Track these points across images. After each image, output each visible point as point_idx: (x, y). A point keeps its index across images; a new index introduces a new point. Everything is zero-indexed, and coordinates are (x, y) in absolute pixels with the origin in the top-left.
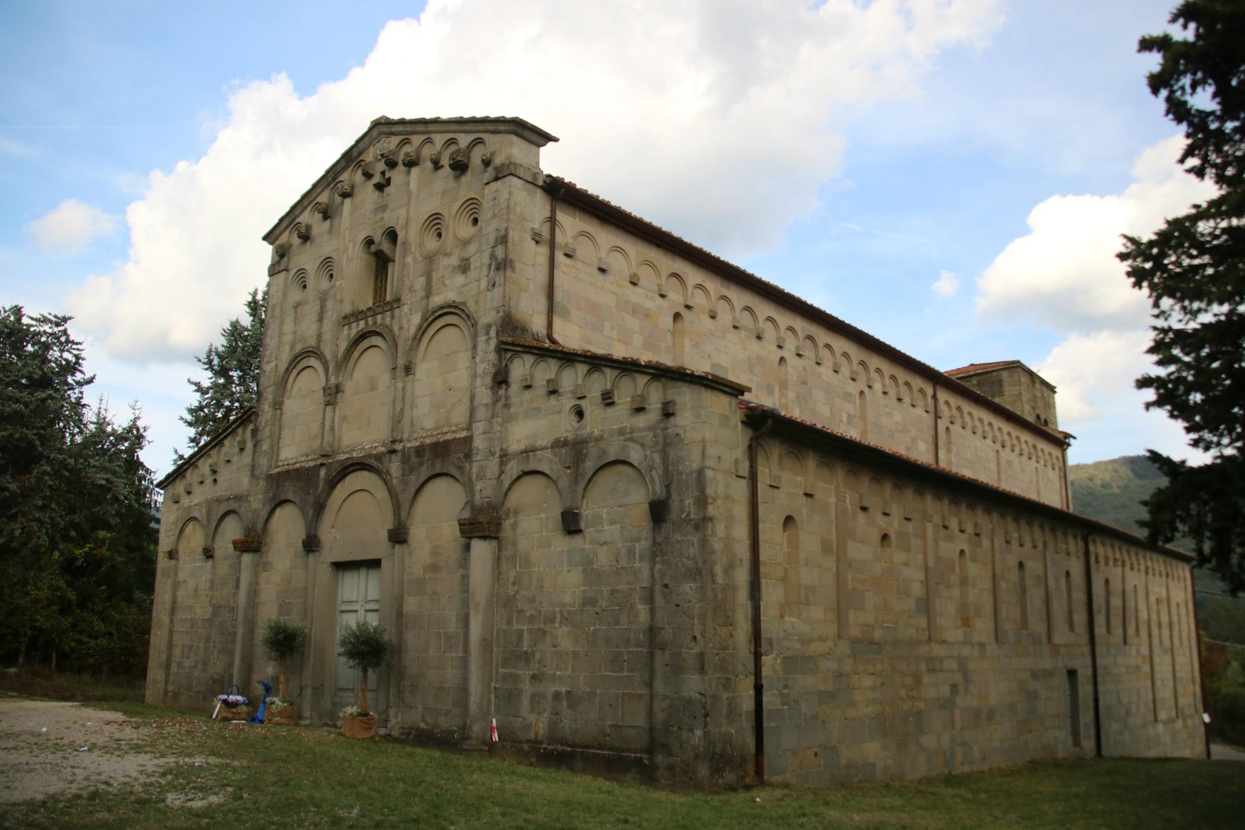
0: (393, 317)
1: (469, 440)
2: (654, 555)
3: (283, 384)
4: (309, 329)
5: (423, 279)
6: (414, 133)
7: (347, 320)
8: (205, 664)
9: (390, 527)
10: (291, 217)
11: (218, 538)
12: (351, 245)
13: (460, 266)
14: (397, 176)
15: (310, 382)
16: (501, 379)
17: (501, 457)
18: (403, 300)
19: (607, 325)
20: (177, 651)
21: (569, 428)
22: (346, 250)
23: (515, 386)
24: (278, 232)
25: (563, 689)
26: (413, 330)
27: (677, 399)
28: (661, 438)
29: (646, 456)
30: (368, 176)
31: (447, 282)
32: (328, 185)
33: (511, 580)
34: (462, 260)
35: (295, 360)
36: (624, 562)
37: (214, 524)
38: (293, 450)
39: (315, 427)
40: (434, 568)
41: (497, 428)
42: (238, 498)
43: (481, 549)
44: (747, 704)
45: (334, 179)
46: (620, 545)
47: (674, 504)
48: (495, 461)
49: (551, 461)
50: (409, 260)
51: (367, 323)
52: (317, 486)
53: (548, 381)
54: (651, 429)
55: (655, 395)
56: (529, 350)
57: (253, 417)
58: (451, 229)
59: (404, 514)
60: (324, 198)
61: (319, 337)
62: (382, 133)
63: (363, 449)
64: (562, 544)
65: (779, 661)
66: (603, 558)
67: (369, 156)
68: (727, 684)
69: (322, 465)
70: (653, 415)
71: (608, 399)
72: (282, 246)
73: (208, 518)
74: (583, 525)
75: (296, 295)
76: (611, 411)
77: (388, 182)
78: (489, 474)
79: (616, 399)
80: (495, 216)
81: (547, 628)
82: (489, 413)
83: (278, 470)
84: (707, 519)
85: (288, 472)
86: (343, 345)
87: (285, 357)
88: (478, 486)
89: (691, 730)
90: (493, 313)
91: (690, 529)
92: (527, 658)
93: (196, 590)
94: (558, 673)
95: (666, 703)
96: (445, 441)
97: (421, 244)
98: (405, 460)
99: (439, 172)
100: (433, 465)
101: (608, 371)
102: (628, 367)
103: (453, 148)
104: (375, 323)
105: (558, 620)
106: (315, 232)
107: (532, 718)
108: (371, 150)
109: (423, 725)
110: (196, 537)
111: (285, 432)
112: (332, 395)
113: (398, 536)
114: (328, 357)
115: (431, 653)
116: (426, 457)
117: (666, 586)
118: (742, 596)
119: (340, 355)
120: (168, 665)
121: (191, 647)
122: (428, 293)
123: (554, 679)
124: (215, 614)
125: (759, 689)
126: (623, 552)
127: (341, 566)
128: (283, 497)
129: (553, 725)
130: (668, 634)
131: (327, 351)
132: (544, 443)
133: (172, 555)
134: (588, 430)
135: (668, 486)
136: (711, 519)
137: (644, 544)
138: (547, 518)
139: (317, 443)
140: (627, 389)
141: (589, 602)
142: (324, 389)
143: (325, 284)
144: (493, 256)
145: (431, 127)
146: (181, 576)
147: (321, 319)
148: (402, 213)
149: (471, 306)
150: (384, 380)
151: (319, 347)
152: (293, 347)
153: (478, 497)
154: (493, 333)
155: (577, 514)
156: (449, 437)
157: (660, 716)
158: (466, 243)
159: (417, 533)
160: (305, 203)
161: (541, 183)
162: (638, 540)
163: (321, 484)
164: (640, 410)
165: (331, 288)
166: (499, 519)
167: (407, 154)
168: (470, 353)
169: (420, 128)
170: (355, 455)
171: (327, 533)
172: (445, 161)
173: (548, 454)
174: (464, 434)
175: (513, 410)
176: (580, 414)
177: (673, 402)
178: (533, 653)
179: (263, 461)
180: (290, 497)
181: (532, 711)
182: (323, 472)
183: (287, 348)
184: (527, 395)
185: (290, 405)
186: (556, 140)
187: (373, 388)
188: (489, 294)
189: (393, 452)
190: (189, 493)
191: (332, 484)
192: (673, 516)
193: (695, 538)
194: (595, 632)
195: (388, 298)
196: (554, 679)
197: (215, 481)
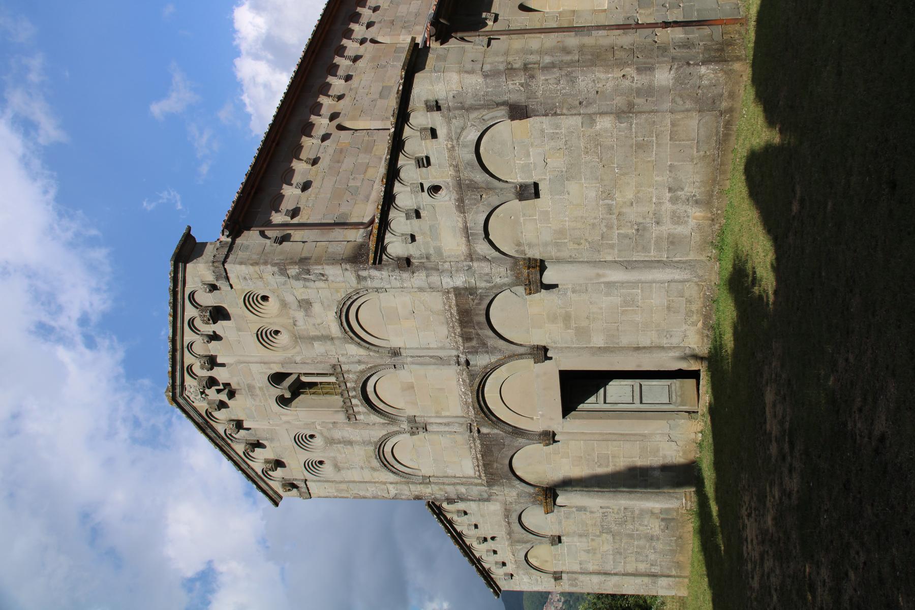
0: (348, 372)
1: (458, 291)
2: (555, 114)
4: (361, 455)
5: (316, 344)
7: (351, 415)
8: (652, 538)
9: (532, 361)
10: (257, 479)
11: (542, 532)
12: (284, 418)
13: (306, 310)
15: (405, 448)
16: (406, 263)
17: (472, 260)
18: (334, 362)
19: (352, 183)
20: (642, 567)
21: (447, 198)
22: (288, 422)
24: (270, 493)
25: (668, 195)
26: (362, 352)
27: (424, 99)
28: (457, 112)
29: (472, 125)
30: (222, 405)
31: (319, 321)
32: (229, 445)
33: (576, 246)
35: (386, 464)
37: (531, 536)
38: (464, 464)
39: (445, 441)
40: (567, 318)
41: (447, 265)
42: (507, 514)
44: (678, 34)
45: (223, 439)
46: (547, 148)
47: (513, 98)
48: (475, 265)
49: (477, 213)
50: (298, 359)
51: (354, 397)
52: (496, 434)
53: (408, 217)
54: (449, 121)
55: (419, 118)
56: (381, 238)
57: (438, 503)
58: (271, 321)
59: (521, 350)
60: (240, 448)
61: (364, 443)
62: (181, 394)
63: (465, 393)
65: (641, 11)
66: (558, 162)
67: (201, 405)
68: (663, 49)
69: (479, 431)
70: (436, 120)
71: (424, 162)
72: (284, 486)
73: (526, 542)
74: (530, 181)
75: (327, 470)
76: (432, 161)
77: (227, 385)
78: (487, 270)
79: (423, 155)
81: (616, 211)
82: (435, 273)
83: (483, 475)
84: (526, 67)
85: (484, 465)
86: (375, 418)
88: (498, 280)
89: (701, 78)
90: (348, 274)
91: (533, 83)
92: (641, 229)
93: (588, 552)
94: (654, 200)
95: (678, 99)
96: (458, 313)
97: (285, 348)
98: (475, 351)
100: (479, 323)
101: (400, 163)
102: (397, 145)
103: (198, 323)
104: (354, 389)
105: (610, 202)
106: (272, 456)
107: (692, 223)
108: (196, 404)
109: (700, 324)
110: (542, 554)
111: (450, 472)
112: (417, 426)
114: (384, 432)
115: (638, 318)
117: (580, 103)
118: (588, 40)
119: (382, 421)
120: (654, 575)
124: (609, 531)
125: (666, 25)
126: (552, 144)
128: (507, 468)
130: (620, 101)
131: (378, 434)
132: (460, 220)
133: (557, 576)
134: (449, 180)
135: (498, 105)
136: (525, 65)
138: (524, 215)
139: (459, 438)
140: (415, 144)
142: (413, 434)
143: (318, 442)
144: (297, 278)
146: (576, 568)
147: (350, 443)
148: (255, 368)
149: (341, 295)
150: (404, 375)
151: (376, 444)
152: (374, 469)
153: (506, 280)
155: (521, 186)
156: (454, 310)
157: (689, 105)
158: (284, 305)
160: (244, 466)
161: (229, 240)
162: (542, 131)
163: (495, 431)
164: (434, 133)
165: (322, 434)
166: (524, 259)
167: (202, 367)
170: (470, 400)
171: (537, 427)
172: (209, 329)
173: (470, 217)
174: (452, 296)
175: (432, 251)
176: (435, 189)
177: (426, 102)
178: (638, 224)
179: (475, 491)
180: (507, 462)
181: (686, 222)
182: (484, 430)
183: (376, 474)
185: (426, 470)
186: (189, 229)
187: (411, 387)
188: (330, 278)
189: (468, 363)
190: (504, 564)
191: (497, 421)
193: (541, 77)
194: (619, 167)
195: (332, 379)
196: (659, 204)
197: (493, 538)
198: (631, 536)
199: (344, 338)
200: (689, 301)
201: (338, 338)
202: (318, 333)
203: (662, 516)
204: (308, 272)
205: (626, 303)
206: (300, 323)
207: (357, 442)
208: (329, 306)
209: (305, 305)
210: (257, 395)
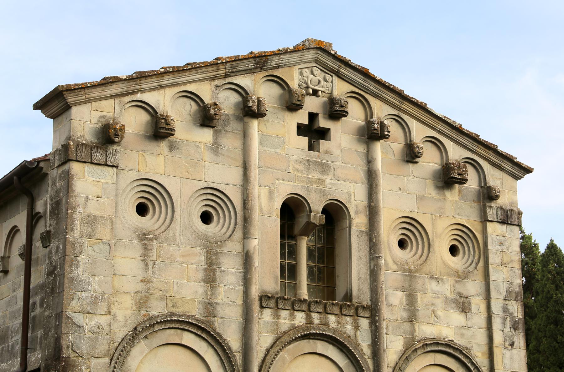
0: (357, 327)
10: (132, 86)
12: (264, 192)
14: (342, 136)
24: (96, 93)
31: (440, 313)
32: (213, 79)
34: (460, 295)
45: (226, 76)
51: (309, 320)
60: (205, 90)
80: (502, 264)
87: (125, 316)
99: (410, 165)
144: (505, 310)
145: (406, 106)
151: (211, 324)
152: (142, 302)
160: (167, 80)
169: (390, 96)
188: (508, 354)
199: (414, 339)
201: (413, 331)
202: (420, 304)
204: (515, 327)
208: (462, 335)
209: (464, 307)
210: (308, 169)
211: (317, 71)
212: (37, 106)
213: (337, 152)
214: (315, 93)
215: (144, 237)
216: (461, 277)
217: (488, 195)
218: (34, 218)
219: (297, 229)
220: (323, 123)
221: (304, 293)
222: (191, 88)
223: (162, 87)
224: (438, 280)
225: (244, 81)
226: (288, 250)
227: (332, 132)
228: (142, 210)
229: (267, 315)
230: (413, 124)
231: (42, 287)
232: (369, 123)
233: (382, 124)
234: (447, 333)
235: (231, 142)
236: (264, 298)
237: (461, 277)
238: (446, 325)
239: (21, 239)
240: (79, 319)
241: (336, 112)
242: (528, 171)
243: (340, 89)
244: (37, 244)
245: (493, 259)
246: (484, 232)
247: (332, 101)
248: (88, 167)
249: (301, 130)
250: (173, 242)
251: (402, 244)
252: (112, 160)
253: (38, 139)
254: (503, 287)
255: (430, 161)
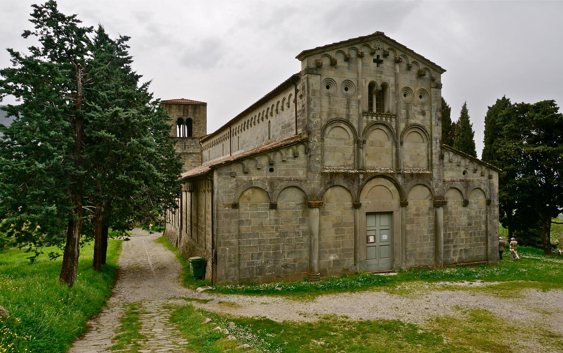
0: (391, 121)
3: (323, 130)
6: (398, 49)
12: (364, 81)
23: (446, 160)
24: (314, 52)
32: (348, 46)
35: (330, 123)
36: (478, 213)
40: (417, 215)
43: (441, 211)
52: (359, 182)
61: (348, 115)
64: (461, 209)
66: (473, 213)
71: (475, 171)
76: (474, 174)
88: (436, 190)
100: (417, 180)
107: (454, 257)
111: (327, 153)
113: (404, 204)
116: (414, 178)
121: (260, 254)
122: (408, 117)
123: (460, 246)
127: (368, 214)
128: (335, 184)
129: (460, 258)
137: (484, 209)
141: (470, 224)
144: (436, 115)
145: (407, 52)
152: (329, 114)
154: (438, 141)
159: (411, 203)
168: (426, 144)
169: (402, 49)
170: (378, 171)
171: (363, 201)
173: (459, 183)
175: (445, 168)
182: (361, 176)
184: (450, 164)
188: (436, 128)
192: (492, 204)
196: (460, 246)
198: (277, 248)
200: (425, 261)
203: (297, 264)
205: (424, 237)
206: (414, 108)
207: (349, 111)
209: (423, 113)
211: (379, 42)
212: (296, 58)
213: (385, 67)
214: (379, 48)
215: (329, 95)
216: (423, 104)
217: (433, 80)
218: (297, 91)
219: (373, 92)
220: (381, 58)
221: (375, 111)
222: (341, 49)
223: (333, 49)
224: (416, 106)
225: (357, 46)
226: (370, 99)
227: (384, 61)
228: (328, 87)
229: (365, 118)
230: (409, 58)
231: (300, 111)
232: (395, 58)
233: (399, 58)
234: (418, 122)
235: (353, 66)
236: (364, 113)
237: (423, 104)
238: (418, 120)
239: (293, 97)
240: (312, 120)
241: (386, 55)
242: (445, 71)
243: (386, 47)
244: (298, 98)
245: (433, 99)
246: (430, 91)
247: (384, 51)
248: (313, 76)
249: (375, 61)
250: (337, 97)
251: (405, 95)
252: (319, 73)
253: (297, 67)
254: (436, 107)
255: (415, 69)
